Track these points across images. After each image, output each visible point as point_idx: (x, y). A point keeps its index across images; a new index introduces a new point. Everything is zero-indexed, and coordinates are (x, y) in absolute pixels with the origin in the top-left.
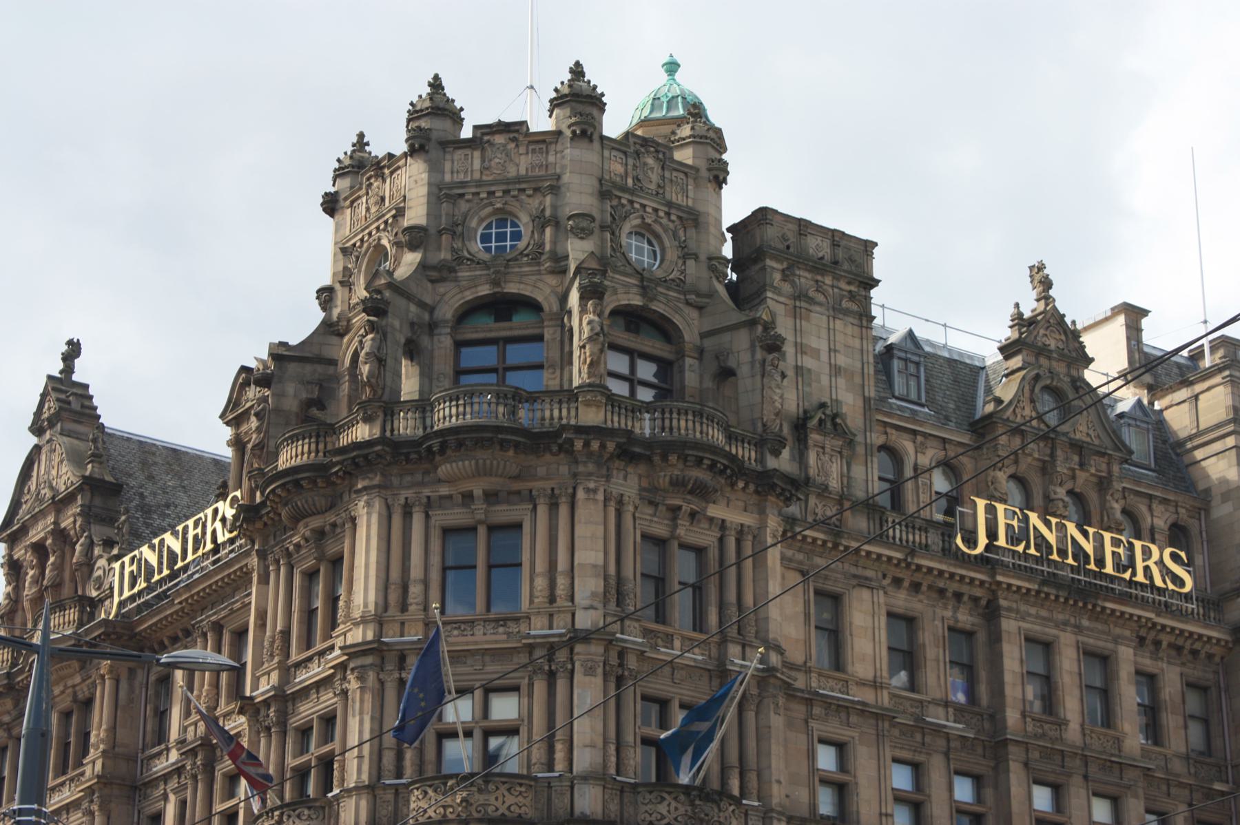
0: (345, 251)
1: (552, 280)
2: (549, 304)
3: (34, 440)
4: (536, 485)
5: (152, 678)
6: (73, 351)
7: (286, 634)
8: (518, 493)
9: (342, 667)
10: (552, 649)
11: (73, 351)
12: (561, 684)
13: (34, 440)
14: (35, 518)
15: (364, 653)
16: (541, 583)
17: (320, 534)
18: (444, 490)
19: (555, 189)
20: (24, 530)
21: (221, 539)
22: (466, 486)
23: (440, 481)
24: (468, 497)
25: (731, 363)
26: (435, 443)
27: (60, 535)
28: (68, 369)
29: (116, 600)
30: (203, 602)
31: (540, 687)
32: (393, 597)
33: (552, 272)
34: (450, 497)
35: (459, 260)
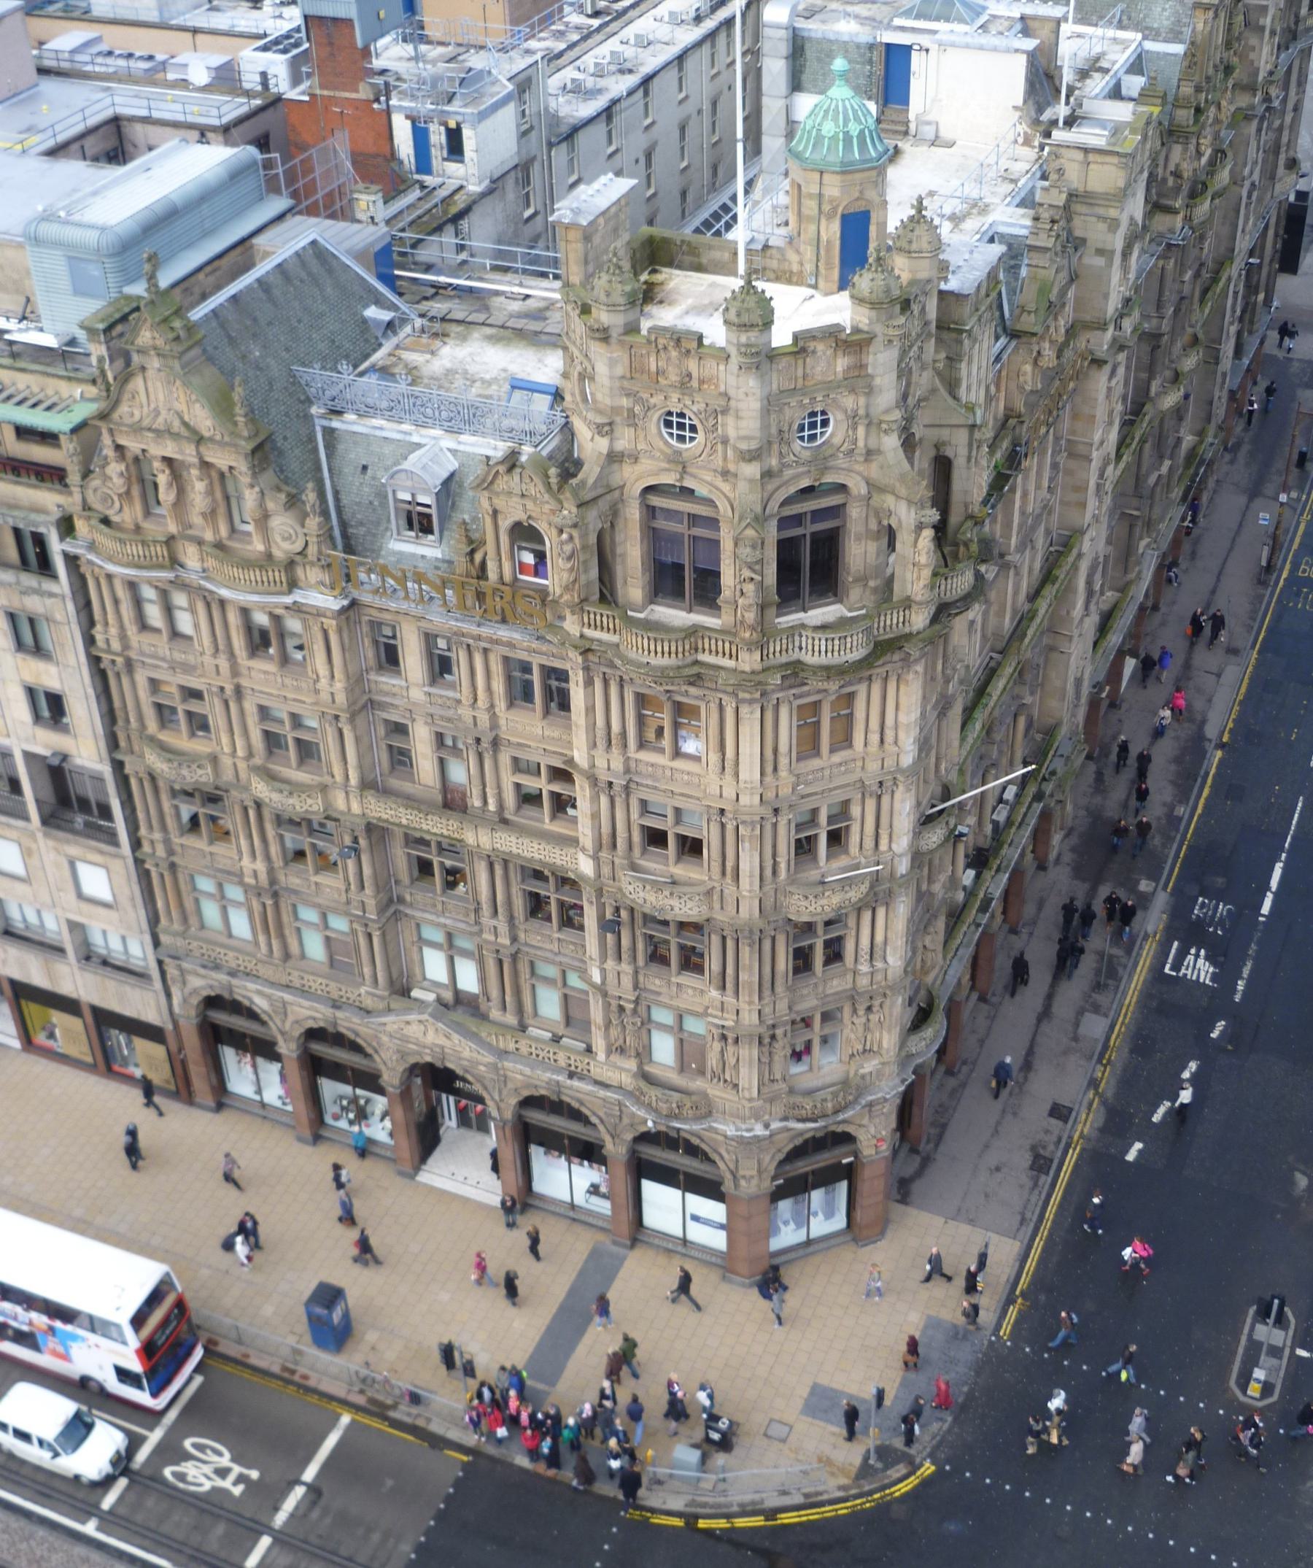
2: (858, 487)
7: (624, 734)
12: (886, 800)
16: (874, 738)
25: (949, 452)
27: (205, 465)
31: (871, 805)
32: (769, 769)
35: (784, 465)
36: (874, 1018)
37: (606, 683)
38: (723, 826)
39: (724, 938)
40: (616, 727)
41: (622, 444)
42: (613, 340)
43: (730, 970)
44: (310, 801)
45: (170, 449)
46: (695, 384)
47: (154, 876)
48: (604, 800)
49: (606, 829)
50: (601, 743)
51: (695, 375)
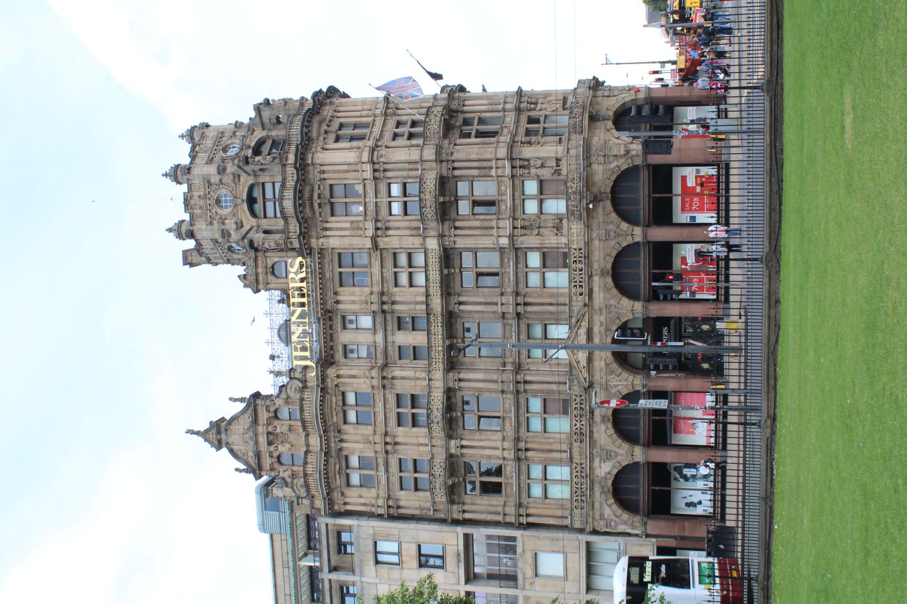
0: (211, 223)
1: (255, 133)
3: (225, 450)
4: (330, 114)
5: (344, 360)
6: (192, 432)
7: (352, 222)
8: (330, 121)
9: (375, 171)
10: (387, 108)
11: (192, 432)
13: (225, 450)
14: (256, 443)
15: (373, 154)
17: (319, 196)
18: (322, 138)
19: (222, 133)
20: (258, 455)
21: (303, 275)
22: (323, 132)
23: (317, 139)
24: (326, 132)
26: (305, 130)
28: (198, 433)
29: (308, 363)
30: (324, 303)
33: (252, 134)
34: (324, 139)
36: (540, 101)
37: (326, 229)
38: (385, 170)
39: (454, 169)
40: (348, 225)
41: (234, 226)
42: (192, 228)
43: (475, 164)
44: (436, 400)
45: (263, 440)
46: (202, 193)
47: (530, 520)
48: (390, 232)
49: (408, 232)
50: (360, 232)
51: (199, 194)
